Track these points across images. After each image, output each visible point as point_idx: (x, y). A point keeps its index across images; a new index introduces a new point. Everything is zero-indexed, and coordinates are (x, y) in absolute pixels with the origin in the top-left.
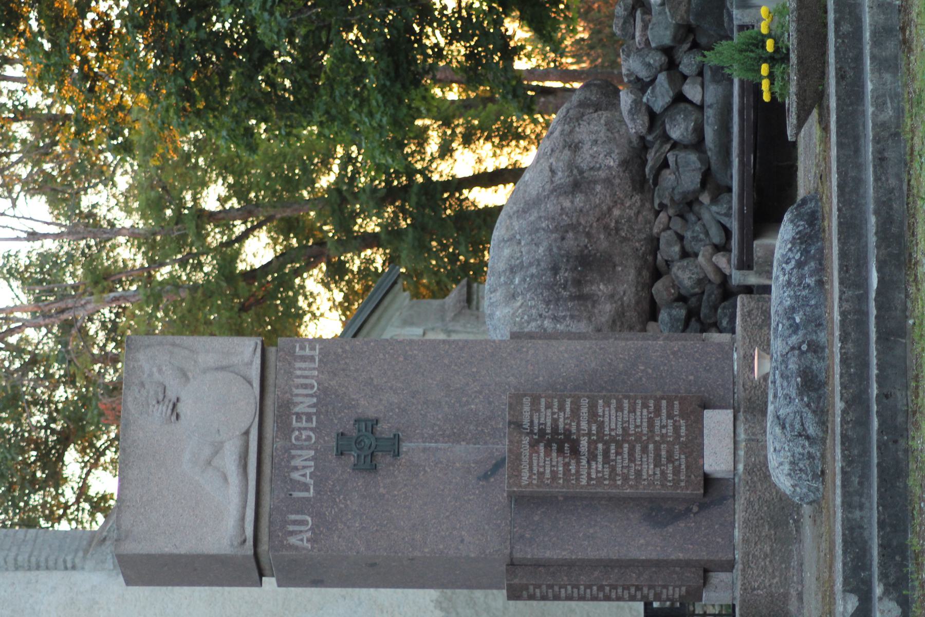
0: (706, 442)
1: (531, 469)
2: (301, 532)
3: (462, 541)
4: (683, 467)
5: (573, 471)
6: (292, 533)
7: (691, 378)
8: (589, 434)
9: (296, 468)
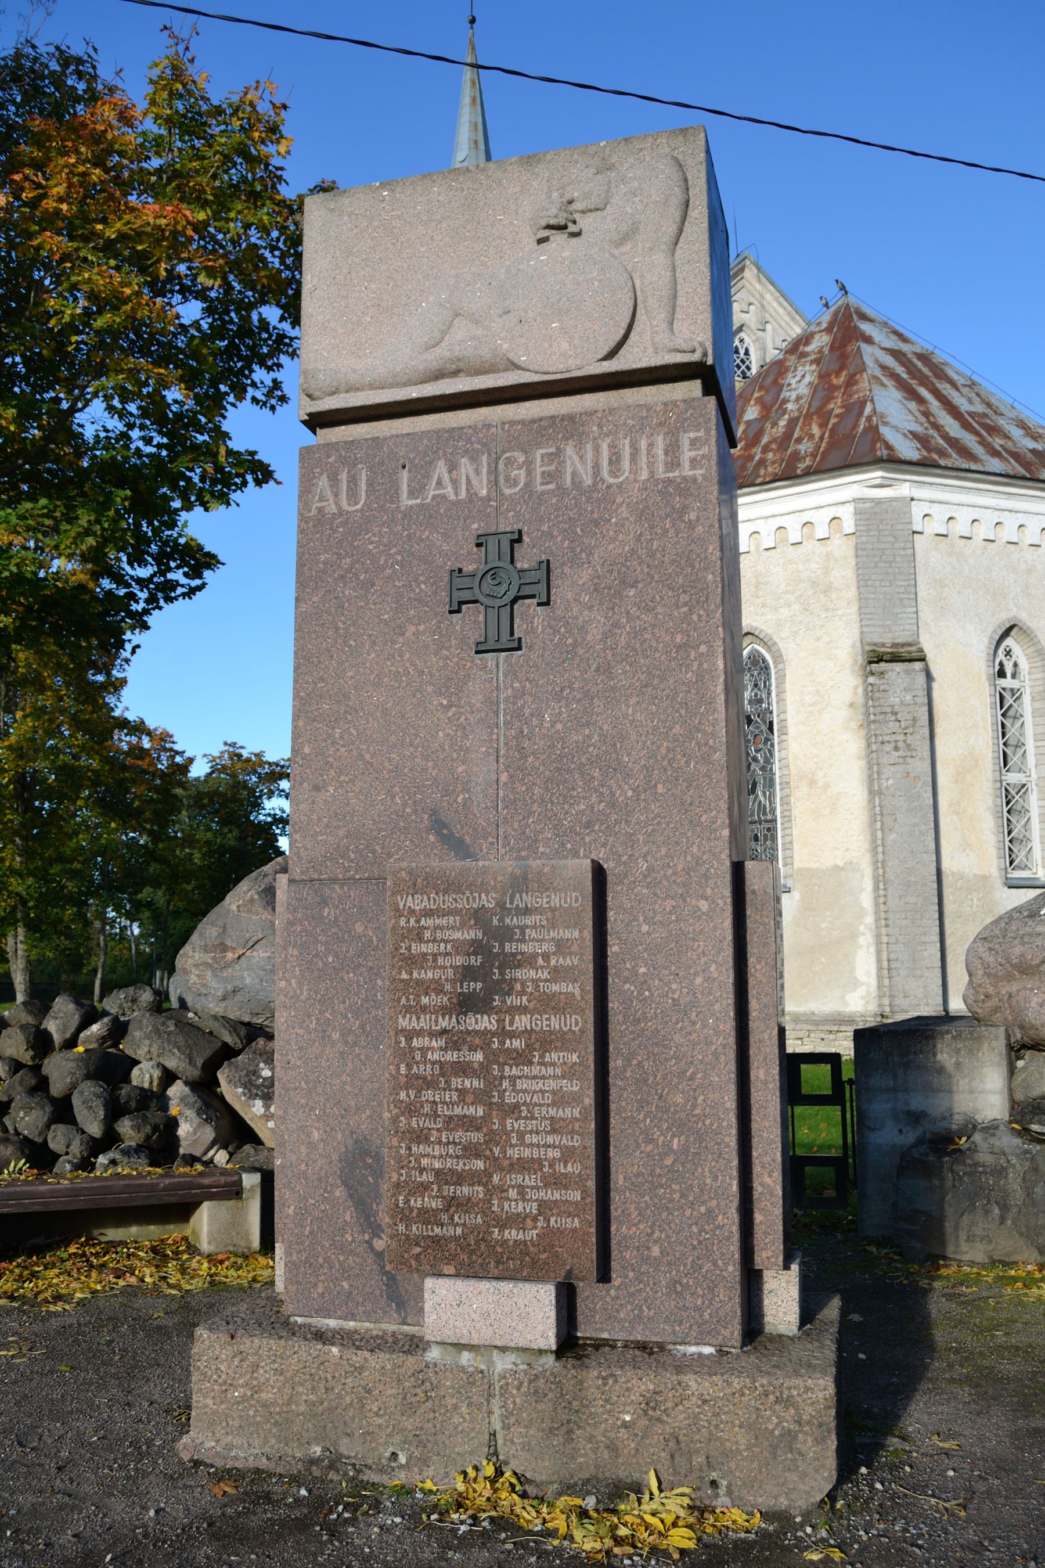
0: (484, 1285)
1: (428, 913)
2: (336, 495)
3: (317, 788)
4: (437, 1230)
5: (425, 1000)
6: (334, 479)
7: (656, 1251)
8: (503, 1034)
9: (452, 467)
